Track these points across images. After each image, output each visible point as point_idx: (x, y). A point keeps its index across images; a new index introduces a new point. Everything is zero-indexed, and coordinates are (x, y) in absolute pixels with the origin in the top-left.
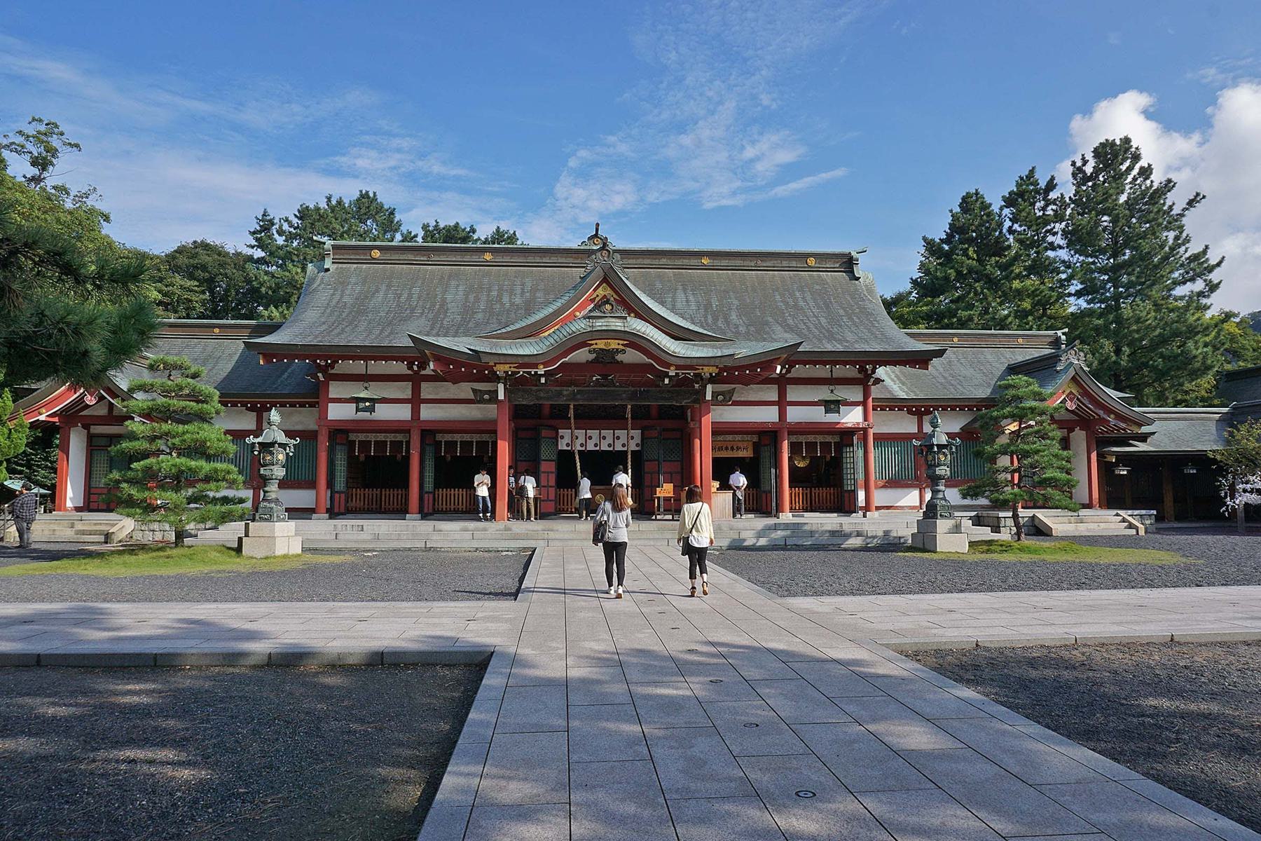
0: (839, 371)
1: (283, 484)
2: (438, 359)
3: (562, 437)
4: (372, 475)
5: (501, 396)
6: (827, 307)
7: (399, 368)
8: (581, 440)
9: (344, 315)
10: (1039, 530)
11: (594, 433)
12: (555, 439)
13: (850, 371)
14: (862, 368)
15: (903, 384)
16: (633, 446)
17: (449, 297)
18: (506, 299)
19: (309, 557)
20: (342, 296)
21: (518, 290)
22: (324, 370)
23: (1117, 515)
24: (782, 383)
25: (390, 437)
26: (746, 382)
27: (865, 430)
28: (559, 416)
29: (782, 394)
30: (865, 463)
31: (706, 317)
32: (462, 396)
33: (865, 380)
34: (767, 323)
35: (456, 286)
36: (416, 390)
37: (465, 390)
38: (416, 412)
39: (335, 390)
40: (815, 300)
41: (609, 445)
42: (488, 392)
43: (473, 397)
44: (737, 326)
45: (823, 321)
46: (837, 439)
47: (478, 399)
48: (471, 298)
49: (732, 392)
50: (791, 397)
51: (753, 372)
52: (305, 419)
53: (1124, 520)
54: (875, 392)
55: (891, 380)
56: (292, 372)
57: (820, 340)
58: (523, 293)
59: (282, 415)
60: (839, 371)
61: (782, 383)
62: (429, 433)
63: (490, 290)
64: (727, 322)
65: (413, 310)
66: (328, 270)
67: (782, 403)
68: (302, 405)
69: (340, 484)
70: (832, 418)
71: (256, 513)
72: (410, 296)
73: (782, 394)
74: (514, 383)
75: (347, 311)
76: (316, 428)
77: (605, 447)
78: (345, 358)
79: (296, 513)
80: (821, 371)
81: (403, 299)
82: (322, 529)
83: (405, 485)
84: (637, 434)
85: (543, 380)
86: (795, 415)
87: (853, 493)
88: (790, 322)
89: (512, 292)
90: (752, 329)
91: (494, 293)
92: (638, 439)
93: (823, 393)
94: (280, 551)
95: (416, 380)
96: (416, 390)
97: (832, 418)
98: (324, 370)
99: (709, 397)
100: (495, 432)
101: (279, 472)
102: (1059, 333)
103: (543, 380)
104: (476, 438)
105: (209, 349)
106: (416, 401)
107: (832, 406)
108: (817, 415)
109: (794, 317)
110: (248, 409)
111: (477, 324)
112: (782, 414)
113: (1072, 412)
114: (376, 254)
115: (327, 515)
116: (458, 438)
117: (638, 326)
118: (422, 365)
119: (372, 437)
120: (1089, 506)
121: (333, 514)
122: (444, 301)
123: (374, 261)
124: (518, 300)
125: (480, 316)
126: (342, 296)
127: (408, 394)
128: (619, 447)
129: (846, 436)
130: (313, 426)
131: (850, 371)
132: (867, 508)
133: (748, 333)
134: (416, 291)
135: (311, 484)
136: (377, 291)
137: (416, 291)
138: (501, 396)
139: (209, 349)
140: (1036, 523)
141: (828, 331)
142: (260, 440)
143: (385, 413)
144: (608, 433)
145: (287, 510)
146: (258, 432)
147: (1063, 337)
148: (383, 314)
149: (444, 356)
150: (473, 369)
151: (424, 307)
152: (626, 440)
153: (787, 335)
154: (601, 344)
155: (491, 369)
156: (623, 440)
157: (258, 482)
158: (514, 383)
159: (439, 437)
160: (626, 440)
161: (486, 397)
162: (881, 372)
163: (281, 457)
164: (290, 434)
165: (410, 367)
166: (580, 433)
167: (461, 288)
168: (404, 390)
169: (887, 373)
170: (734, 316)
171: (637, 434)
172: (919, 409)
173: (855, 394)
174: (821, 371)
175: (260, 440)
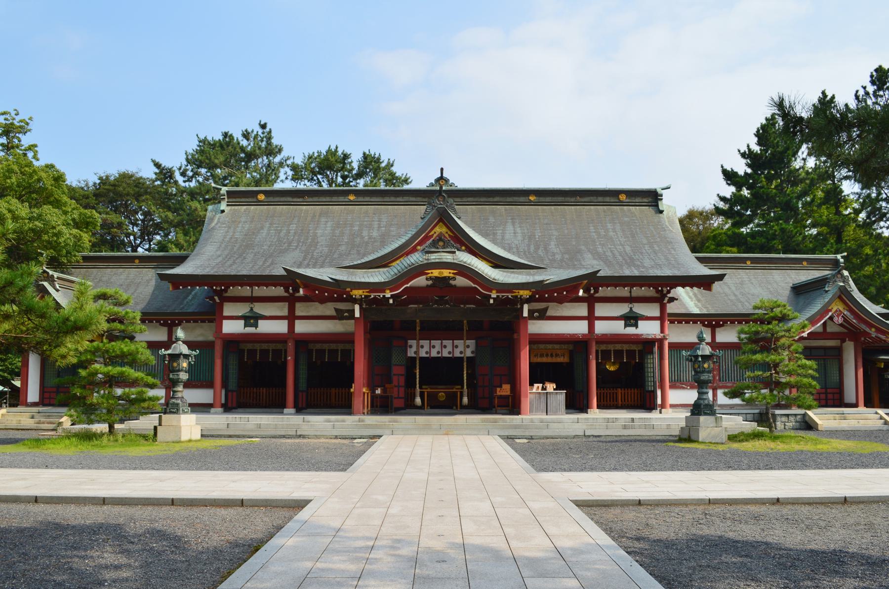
0: (637, 291)
1: (188, 385)
2: (305, 287)
3: (411, 347)
4: (255, 378)
5: (357, 315)
6: (633, 236)
7: (279, 291)
9: (235, 249)
10: (808, 425)
11: (436, 343)
13: (650, 292)
14: (660, 288)
15: (699, 300)
16: (469, 353)
17: (319, 232)
18: (365, 233)
19: (209, 443)
21: (376, 224)
22: (219, 293)
23: (876, 413)
24: (591, 301)
25: (272, 347)
26: (561, 301)
27: (661, 341)
28: (408, 330)
29: (591, 310)
30: (663, 366)
31: (529, 246)
34: (579, 251)
35: (326, 222)
36: (292, 309)
37: (328, 309)
38: (291, 326)
39: (229, 309)
40: (623, 230)
41: (449, 353)
42: (348, 311)
43: (334, 313)
44: (554, 254)
45: (628, 249)
46: (640, 347)
47: (340, 316)
48: (337, 232)
51: (564, 291)
52: (204, 333)
53: (881, 418)
54: (671, 308)
55: (687, 300)
56: (196, 294)
57: (621, 266)
58: (379, 227)
59: (183, 329)
60: (637, 291)
61: (591, 301)
62: (304, 342)
63: (352, 226)
64: (545, 248)
65: (290, 244)
66: (223, 211)
67: (591, 318)
68: (203, 321)
69: (233, 385)
70: (631, 330)
71: (170, 407)
72: (288, 232)
73: (591, 310)
74: (368, 304)
75: (238, 245)
76: (213, 339)
77: (445, 354)
79: (197, 408)
80: (624, 292)
81: (282, 234)
82: (218, 420)
83: (284, 385)
84: (471, 343)
85: (391, 301)
86: (601, 328)
87: (654, 393)
88: (600, 250)
89: (370, 227)
90: (567, 256)
91: (356, 228)
93: (622, 309)
94: (185, 437)
95: (292, 301)
96: (292, 309)
97: (631, 330)
98: (219, 293)
100: (353, 342)
101: (184, 376)
102: (839, 256)
103: (391, 301)
104: (340, 347)
105: (132, 276)
106: (291, 318)
107: (631, 319)
108: (619, 328)
109: (603, 245)
110: (161, 325)
111: (341, 255)
112: (591, 327)
113: (841, 325)
114: (261, 197)
115: (220, 410)
116: (326, 346)
118: (295, 289)
119: (258, 347)
120: (856, 405)
121: (228, 408)
122: (315, 234)
123: (259, 203)
124: (375, 234)
125: (343, 248)
127: (285, 312)
128: (457, 354)
129: (648, 345)
130: (211, 338)
131: (650, 292)
132: (663, 406)
133: (562, 260)
134: (293, 227)
135: (209, 385)
136: (262, 228)
137: (293, 227)
138: (357, 315)
139: (132, 276)
140: (807, 419)
141: (631, 259)
142: (169, 352)
143: (266, 327)
145: (191, 405)
146: (167, 345)
147: (842, 260)
148: (265, 247)
150: (335, 292)
151: (299, 241)
152: (462, 348)
153: (595, 262)
155: (348, 294)
156: (461, 348)
157: (170, 385)
158: (368, 304)
159: (311, 346)
160: (462, 348)
162: (680, 292)
163: (185, 365)
164: (191, 345)
165: (287, 291)
167: (329, 224)
168: (282, 309)
169: (687, 293)
170: (552, 246)
172: (713, 322)
173: (653, 310)
174: (624, 292)
175: (169, 352)
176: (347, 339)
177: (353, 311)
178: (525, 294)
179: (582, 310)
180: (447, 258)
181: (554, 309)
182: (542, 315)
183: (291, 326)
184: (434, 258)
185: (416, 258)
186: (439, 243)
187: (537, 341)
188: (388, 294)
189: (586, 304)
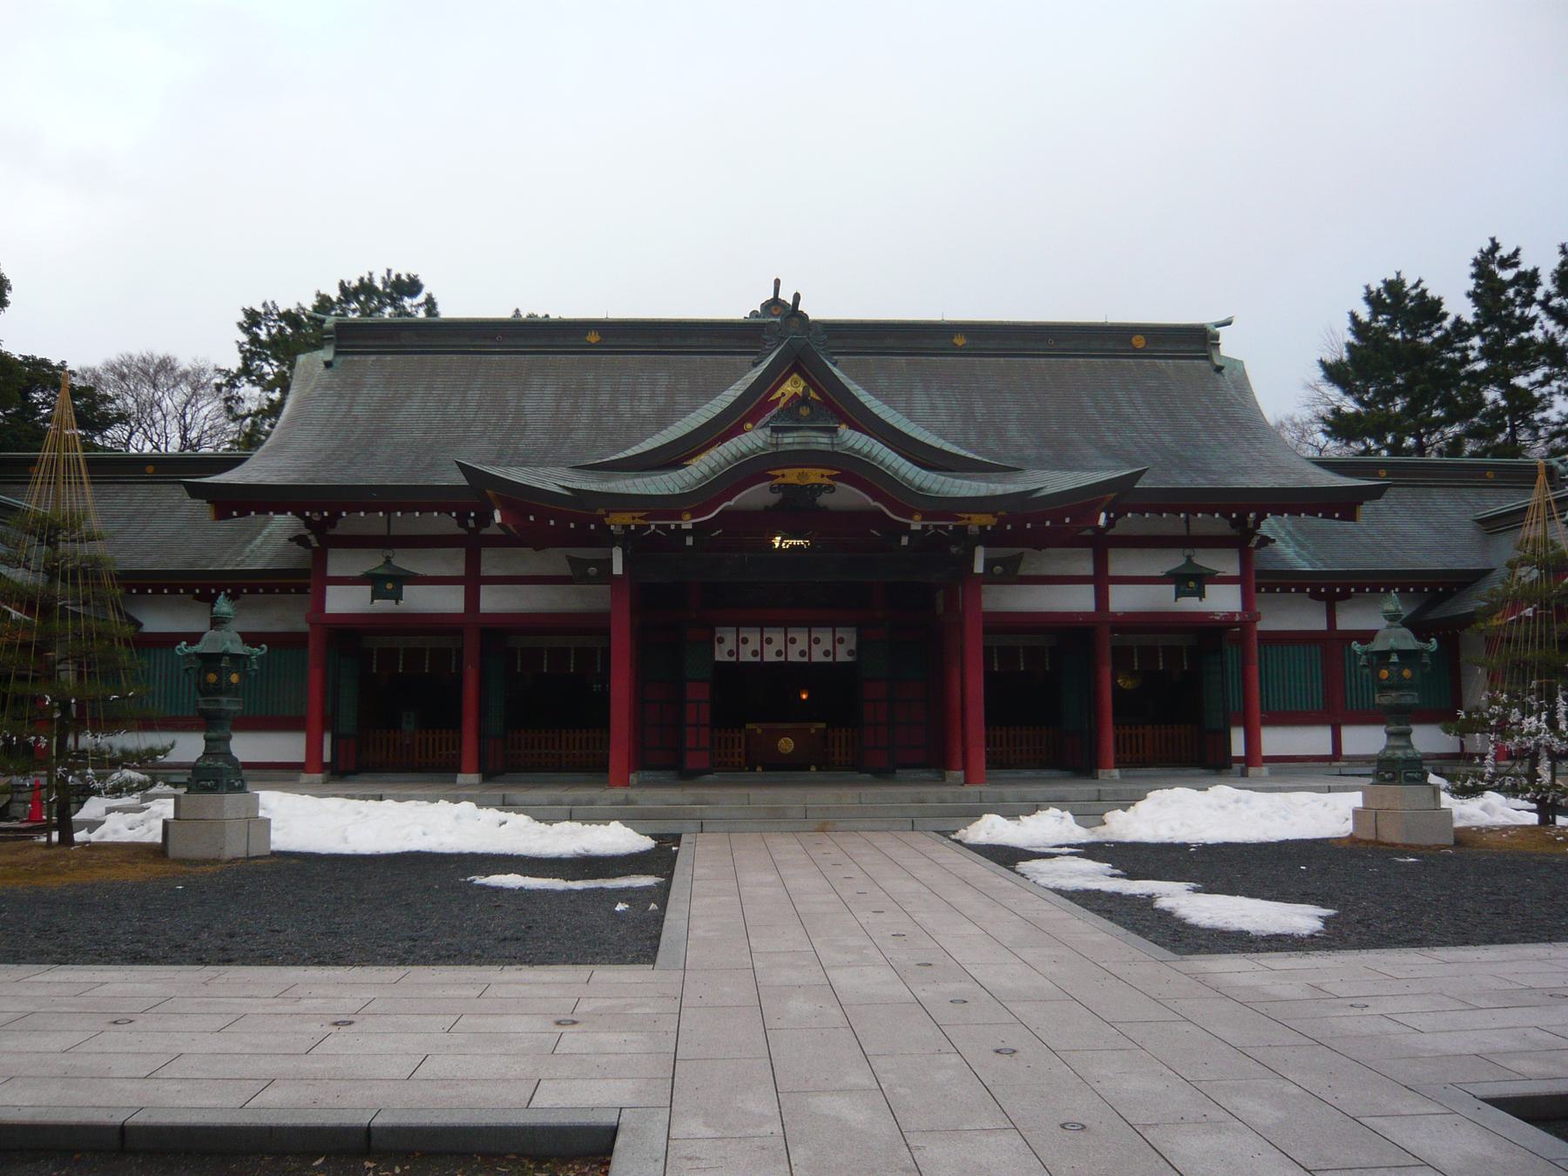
3: (721, 640)
5: (618, 569)
7: (444, 523)
12: (710, 643)
13: (1216, 524)
20: (351, 406)
24: (1101, 545)
29: (1101, 563)
32: (549, 570)
33: (1243, 540)
36: (473, 562)
37: (554, 561)
38: (472, 599)
43: (565, 570)
45: (1167, 439)
47: (576, 576)
49: (1016, 561)
50: (1115, 569)
56: (270, 534)
61: (1101, 545)
67: (1101, 581)
70: (1190, 604)
73: (1101, 563)
77: (794, 657)
78: (353, 508)
80: (1169, 524)
85: (689, 541)
86: (1123, 599)
88: (1110, 438)
93: (1171, 561)
95: (473, 544)
96: (473, 562)
99: (979, 568)
100: (605, 632)
103: (689, 541)
106: (472, 582)
108: (1162, 598)
110: (198, 598)
112: (1102, 598)
117: (855, 440)
118: (482, 515)
124: (644, 408)
126: (351, 406)
127: (458, 569)
130: (302, 626)
131: (1216, 524)
138: (618, 569)
143: (421, 600)
148: (417, 434)
149: (519, 499)
161: (592, 570)
165: (462, 520)
173: (1229, 564)
174: (1169, 524)
176: (592, 626)
177: (610, 561)
183: (472, 599)
188: (687, 525)
189: (1090, 550)
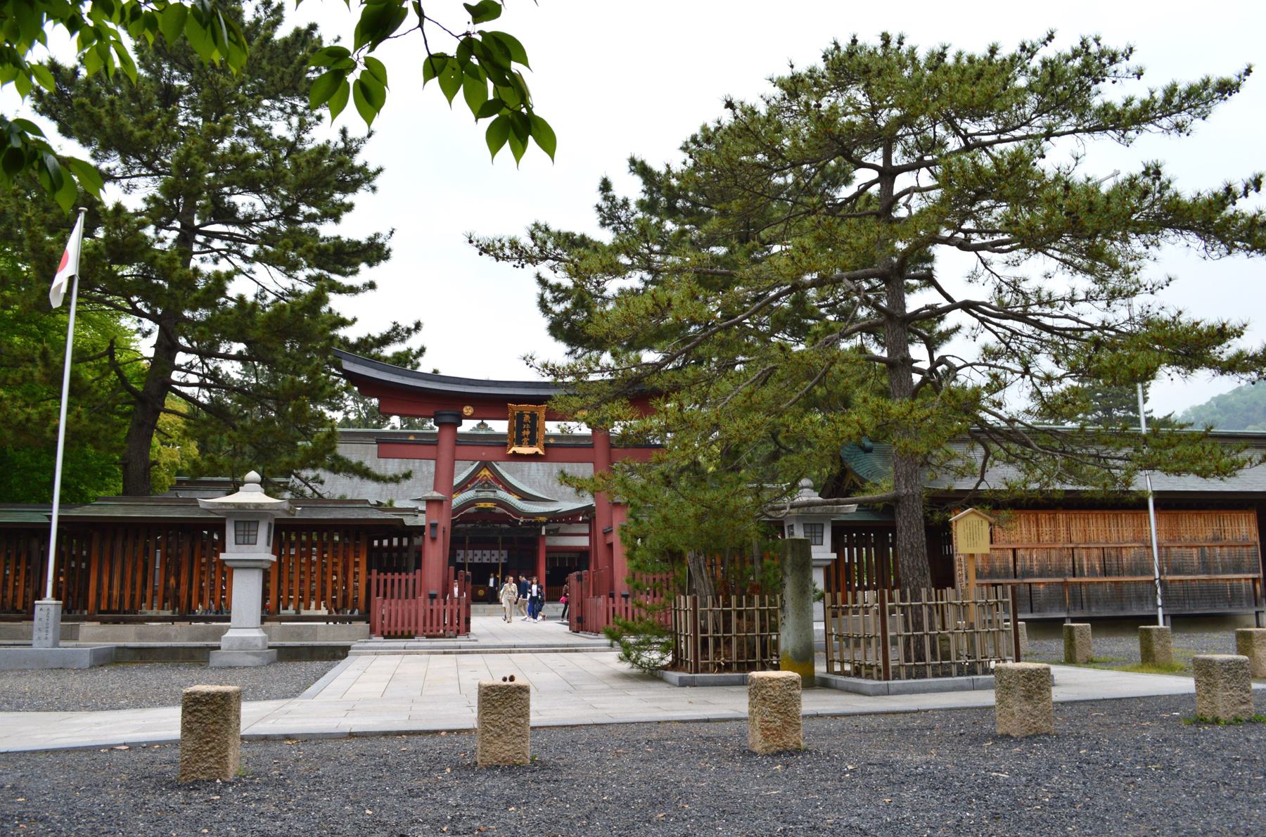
8: (471, 556)
11: (479, 552)
26: (570, 523)
77: (485, 561)
84: (505, 552)
92: (505, 556)
128: (494, 561)
144: (487, 552)
152: (497, 556)
154: (482, 505)
156: (497, 556)
166: (470, 552)
171: (505, 552)
178: (543, 519)
179: (586, 529)
180: (491, 495)
181: (564, 528)
182: (556, 533)
184: (482, 495)
185: (469, 495)
186: (486, 485)
187: (551, 550)
